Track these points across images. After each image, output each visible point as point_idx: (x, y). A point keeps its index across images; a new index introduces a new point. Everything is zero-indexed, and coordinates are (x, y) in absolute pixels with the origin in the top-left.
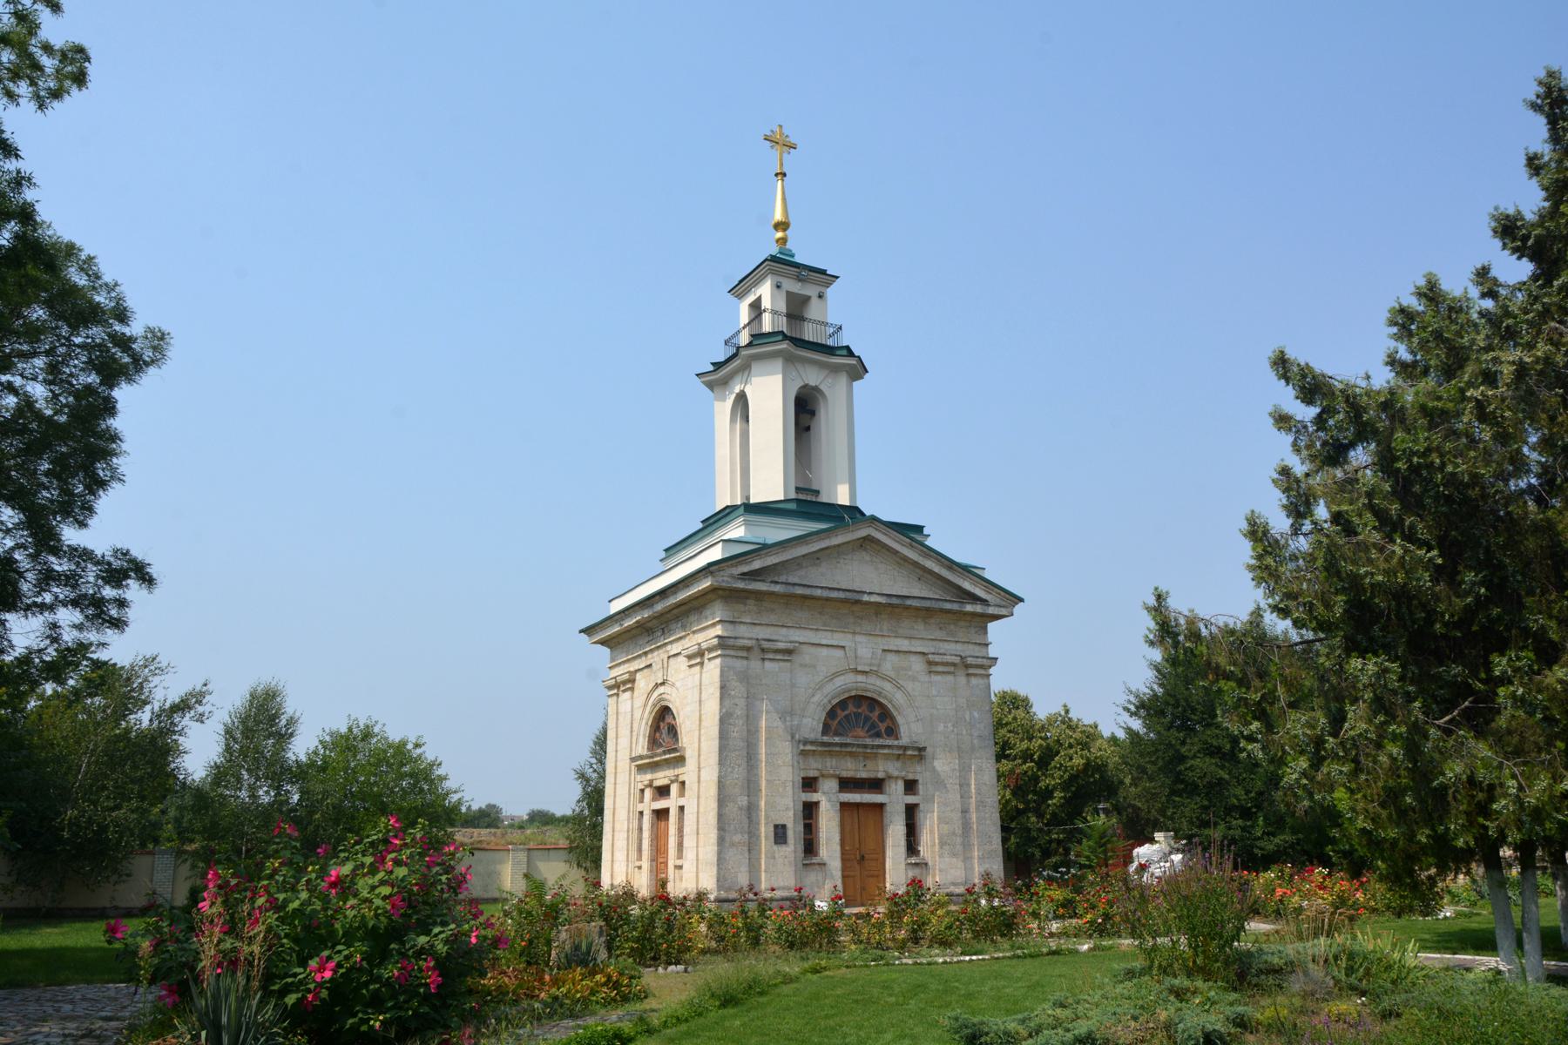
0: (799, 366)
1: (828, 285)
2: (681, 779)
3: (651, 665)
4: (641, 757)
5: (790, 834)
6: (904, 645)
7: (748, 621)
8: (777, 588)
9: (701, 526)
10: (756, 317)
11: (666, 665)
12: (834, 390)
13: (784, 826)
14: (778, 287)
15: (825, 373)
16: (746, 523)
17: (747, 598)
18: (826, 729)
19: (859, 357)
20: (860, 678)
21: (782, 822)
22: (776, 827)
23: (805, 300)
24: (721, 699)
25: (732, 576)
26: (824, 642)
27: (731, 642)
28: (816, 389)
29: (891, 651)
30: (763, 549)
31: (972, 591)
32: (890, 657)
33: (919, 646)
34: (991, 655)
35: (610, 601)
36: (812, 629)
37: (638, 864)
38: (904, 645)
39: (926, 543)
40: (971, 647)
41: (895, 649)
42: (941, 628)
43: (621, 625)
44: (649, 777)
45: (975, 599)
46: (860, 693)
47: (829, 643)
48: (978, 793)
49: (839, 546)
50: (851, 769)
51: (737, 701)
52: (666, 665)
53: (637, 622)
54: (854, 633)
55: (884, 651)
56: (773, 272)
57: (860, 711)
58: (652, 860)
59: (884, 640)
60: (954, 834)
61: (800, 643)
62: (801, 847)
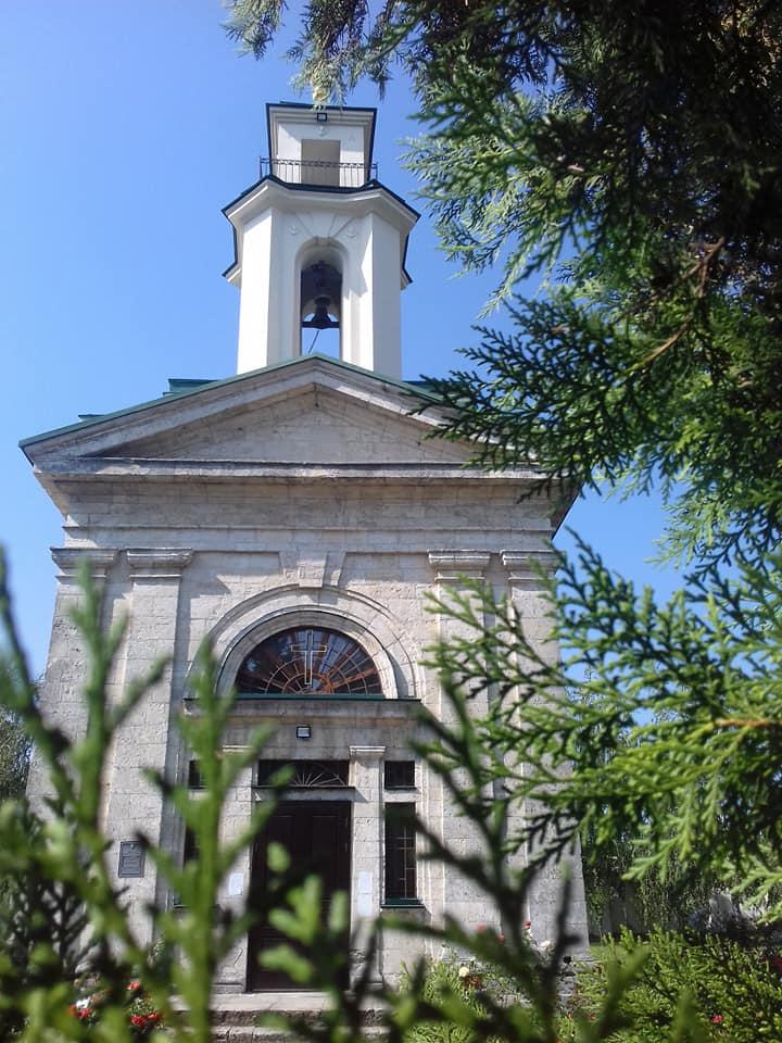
0: (304, 218)
6: (387, 542)
7: (109, 525)
8: (144, 471)
15: (341, 223)
17: (112, 493)
20: (306, 600)
24: (52, 643)
25: (70, 459)
26: (241, 548)
28: (332, 244)
29: (364, 554)
38: (387, 542)
40: (515, 537)
41: (371, 550)
42: (457, 514)
47: (251, 548)
59: (351, 538)
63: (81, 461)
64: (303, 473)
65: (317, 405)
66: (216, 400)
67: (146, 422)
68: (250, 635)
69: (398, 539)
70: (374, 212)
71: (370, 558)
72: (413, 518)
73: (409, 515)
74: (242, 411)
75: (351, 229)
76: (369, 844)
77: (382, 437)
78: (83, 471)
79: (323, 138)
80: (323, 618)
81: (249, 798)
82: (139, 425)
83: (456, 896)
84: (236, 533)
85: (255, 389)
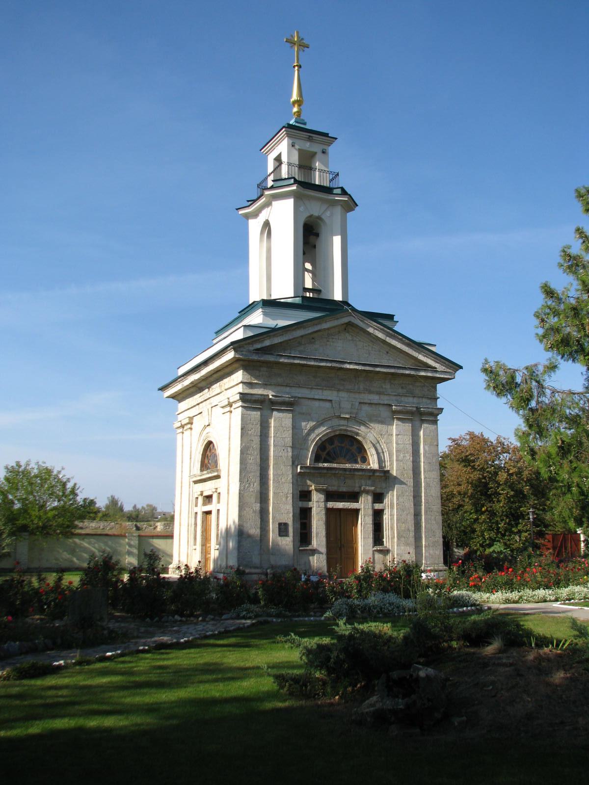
1: (330, 144)
2: (218, 491)
3: (201, 413)
4: (195, 476)
5: (291, 530)
6: (375, 398)
9: (239, 314)
10: (279, 166)
11: (210, 413)
12: (331, 217)
13: (286, 525)
14: (293, 146)
15: (324, 207)
16: (265, 314)
18: (317, 458)
19: (350, 195)
21: (284, 521)
22: (280, 524)
23: (313, 155)
25: (249, 351)
26: (316, 397)
27: (249, 397)
28: (319, 218)
29: (366, 403)
30: (273, 331)
31: (425, 361)
32: (366, 408)
33: (385, 400)
34: (439, 406)
35: (178, 369)
36: (308, 388)
37: (194, 547)
39: (395, 328)
41: (369, 402)
43: (182, 385)
44: (200, 487)
45: (427, 367)
46: (342, 433)
48: (427, 502)
49: (328, 329)
50: (336, 485)
51: (253, 438)
52: (210, 413)
53: (192, 383)
54: (339, 390)
55: (360, 403)
56: (289, 135)
57: (343, 445)
58: (202, 545)
60: (408, 530)
61: (300, 398)
62: (298, 538)
63: (255, 353)
65: (345, 329)
67: (280, 335)
69: (380, 397)
70: (341, 205)
71: (368, 405)
73: (384, 387)
75: (329, 212)
76: (369, 525)
77: (372, 348)
78: (255, 357)
79: (308, 149)
81: (324, 506)
82: (277, 337)
85: (326, 322)
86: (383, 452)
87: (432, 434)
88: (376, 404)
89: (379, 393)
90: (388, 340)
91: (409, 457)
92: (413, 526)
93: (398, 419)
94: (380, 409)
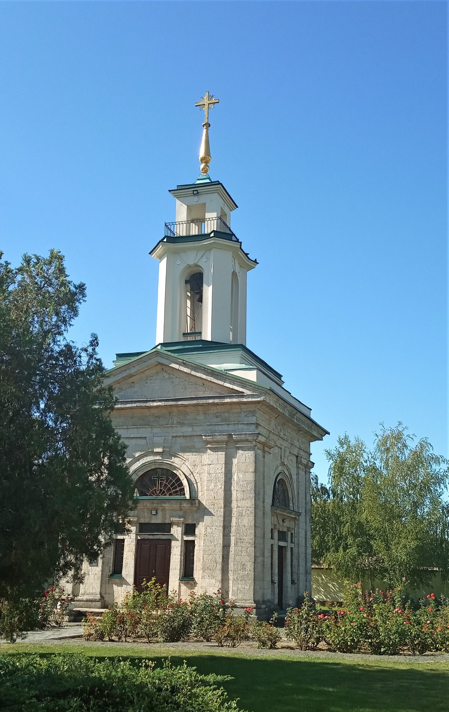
6: (187, 430)
15: (200, 254)
41: (182, 434)
54: (152, 427)
55: (172, 436)
64: (152, 404)
66: (119, 373)
68: (136, 473)
72: (199, 419)
73: (197, 418)
74: (131, 376)
80: (164, 465)
81: (135, 538)
83: (205, 577)
84: (131, 430)
86: (197, 483)
87: (248, 460)
88: (190, 436)
89: (191, 425)
90: (193, 373)
91: (220, 486)
92: (221, 558)
93: (211, 449)
94: (195, 441)
